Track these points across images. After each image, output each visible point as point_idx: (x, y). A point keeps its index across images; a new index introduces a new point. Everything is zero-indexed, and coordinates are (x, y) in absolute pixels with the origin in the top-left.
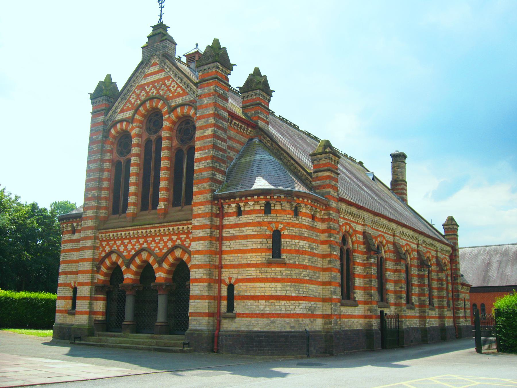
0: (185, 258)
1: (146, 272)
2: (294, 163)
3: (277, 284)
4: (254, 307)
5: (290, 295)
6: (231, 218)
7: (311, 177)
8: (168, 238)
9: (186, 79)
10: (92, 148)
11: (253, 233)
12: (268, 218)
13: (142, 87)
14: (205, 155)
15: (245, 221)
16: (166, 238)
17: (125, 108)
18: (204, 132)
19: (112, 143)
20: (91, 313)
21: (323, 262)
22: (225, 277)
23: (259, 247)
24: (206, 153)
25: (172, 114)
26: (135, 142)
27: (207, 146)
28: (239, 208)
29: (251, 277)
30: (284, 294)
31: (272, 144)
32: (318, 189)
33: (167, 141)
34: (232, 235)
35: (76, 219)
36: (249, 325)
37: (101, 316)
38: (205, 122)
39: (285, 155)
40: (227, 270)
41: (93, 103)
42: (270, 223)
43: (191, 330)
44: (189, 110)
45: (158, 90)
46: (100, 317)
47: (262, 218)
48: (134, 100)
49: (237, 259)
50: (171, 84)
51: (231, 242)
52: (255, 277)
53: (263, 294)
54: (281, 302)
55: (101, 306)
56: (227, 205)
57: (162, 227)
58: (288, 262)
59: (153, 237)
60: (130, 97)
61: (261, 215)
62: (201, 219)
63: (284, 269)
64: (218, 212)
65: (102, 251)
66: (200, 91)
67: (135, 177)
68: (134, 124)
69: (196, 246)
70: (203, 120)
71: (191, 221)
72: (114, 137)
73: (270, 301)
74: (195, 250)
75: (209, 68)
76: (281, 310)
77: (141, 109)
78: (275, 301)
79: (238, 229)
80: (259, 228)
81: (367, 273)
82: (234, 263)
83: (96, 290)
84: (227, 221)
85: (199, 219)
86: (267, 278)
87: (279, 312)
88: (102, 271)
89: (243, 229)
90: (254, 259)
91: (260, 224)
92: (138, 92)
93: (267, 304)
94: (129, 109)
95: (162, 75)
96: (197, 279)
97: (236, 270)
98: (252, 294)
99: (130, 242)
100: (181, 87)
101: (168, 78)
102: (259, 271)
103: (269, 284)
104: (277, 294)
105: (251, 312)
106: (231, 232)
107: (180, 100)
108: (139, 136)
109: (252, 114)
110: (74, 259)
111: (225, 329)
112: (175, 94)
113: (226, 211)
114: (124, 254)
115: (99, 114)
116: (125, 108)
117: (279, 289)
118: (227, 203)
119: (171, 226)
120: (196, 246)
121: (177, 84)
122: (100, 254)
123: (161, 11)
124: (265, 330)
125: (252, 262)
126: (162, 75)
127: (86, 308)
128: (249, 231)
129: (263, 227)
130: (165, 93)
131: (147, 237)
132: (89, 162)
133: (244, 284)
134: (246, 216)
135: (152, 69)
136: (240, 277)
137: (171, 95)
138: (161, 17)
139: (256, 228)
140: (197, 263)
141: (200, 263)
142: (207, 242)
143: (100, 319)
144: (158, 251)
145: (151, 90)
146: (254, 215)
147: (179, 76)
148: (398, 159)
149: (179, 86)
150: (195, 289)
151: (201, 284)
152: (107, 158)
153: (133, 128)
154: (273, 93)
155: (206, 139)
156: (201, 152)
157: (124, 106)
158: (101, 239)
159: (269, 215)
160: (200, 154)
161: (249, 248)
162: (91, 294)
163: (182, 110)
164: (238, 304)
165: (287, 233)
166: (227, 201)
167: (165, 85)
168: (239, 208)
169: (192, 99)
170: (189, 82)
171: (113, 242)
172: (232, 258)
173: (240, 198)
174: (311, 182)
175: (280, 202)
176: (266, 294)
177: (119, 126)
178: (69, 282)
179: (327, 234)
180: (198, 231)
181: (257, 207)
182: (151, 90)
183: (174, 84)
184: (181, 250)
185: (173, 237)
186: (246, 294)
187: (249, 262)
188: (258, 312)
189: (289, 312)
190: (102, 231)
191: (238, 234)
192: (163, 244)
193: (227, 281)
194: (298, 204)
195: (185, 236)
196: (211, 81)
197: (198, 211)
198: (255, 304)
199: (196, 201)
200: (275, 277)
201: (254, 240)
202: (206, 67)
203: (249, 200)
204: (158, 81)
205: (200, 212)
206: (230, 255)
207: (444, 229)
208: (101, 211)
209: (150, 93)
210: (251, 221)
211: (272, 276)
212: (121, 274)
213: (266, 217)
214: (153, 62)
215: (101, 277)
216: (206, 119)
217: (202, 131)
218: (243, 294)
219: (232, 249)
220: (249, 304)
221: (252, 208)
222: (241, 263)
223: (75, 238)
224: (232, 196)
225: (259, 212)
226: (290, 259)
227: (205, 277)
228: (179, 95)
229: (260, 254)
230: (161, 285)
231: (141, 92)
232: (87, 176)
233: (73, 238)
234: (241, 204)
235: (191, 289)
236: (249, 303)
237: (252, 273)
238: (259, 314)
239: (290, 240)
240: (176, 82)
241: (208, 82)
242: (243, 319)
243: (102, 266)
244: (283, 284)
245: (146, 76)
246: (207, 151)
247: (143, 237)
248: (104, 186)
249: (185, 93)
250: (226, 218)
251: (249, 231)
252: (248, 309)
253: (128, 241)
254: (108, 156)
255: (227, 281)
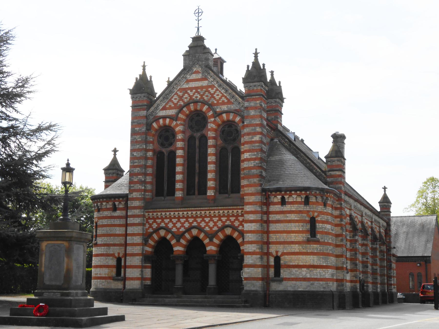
0: (235, 235)
1: (196, 245)
2: (310, 162)
3: (314, 256)
4: (298, 273)
5: (323, 264)
6: (276, 206)
7: (326, 174)
8: (217, 219)
9: (232, 91)
10: (135, 139)
11: (296, 219)
12: (307, 208)
13: (185, 91)
14: (254, 157)
15: (289, 210)
16: (215, 219)
17: (167, 106)
18: (252, 138)
19: (154, 135)
20: (142, 279)
21: (336, 240)
22: (272, 251)
23: (301, 229)
24: (254, 155)
25: (217, 118)
26: (180, 138)
27: (255, 150)
28: (283, 198)
29: (296, 251)
30: (319, 264)
31: (290, 145)
32: (332, 184)
33: (213, 140)
34: (278, 219)
35: (119, 199)
36: (294, 287)
37: (149, 282)
38: (252, 130)
39: (302, 154)
40: (274, 245)
41: (132, 98)
42: (308, 212)
43: (246, 291)
44: (235, 117)
45: (202, 96)
46: (148, 282)
47: (302, 207)
48: (177, 100)
49: (283, 237)
50: (215, 92)
51: (277, 224)
52: (298, 251)
53: (305, 264)
54: (317, 269)
55: (149, 273)
56: (273, 197)
57: (212, 210)
58: (321, 241)
59: (203, 218)
60: (172, 98)
61: (302, 206)
62: (252, 206)
63: (318, 246)
64: (265, 201)
65: (149, 228)
66: (246, 104)
67: (181, 167)
68: (179, 122)
69: (247, 227)
70: (251, 128)
71: (242, 207)
72: (156, 130)
73: (310, 269)
74: (247, 230)
75: (255, 86)
76: (317, 276)
77: (185, 109)
78: (313, 269)
79: (283, 215)
80: (301, 215)
81: (353, 247)
82: (280, 240)
83: (145, 260)
84: (273, 208)
85: (250, 206)
86: (307, 252)
87: (316, 277)
88: (150, 244)
89: (288, 215)
90: (297, 238)
91: (301, 212)
92: (181, 94)
93: (308, 271)
94: (171, 108)
95: (205, 83)
96: (250, 252)
97: (282, 245)
98: (296, 264)
99: (179, 221)
100: (226, 97)
101: (212, 87)
102: (301, 247)
103: (309, 256)
104: (314, 264)
105: (296, 277)
106: (276, 217)
107: (225, 108)
108: (183, 132)
109: (272, 118)
110: (117, 233)
111: (274, 289)
112: (220, 102)
113: (272, 201)
114: (173, 230)
115: (140, 109)
116: (167, 106)
117: (316, 260)
118: (273, 195)
119: (221, 210)
120: (247, 227)
121: (221, 93)
122: (147, 229)
123: (198, 24)
124: (307, 290)
125: (295, 240)
126: (205, 83)
127: (138, 275)
128: (293, 217)
129: (304, 215)
130: (209, 100)
131: (197, 217)
132: (132, 151)
133: (289, 256)
134: (289, 206)
135: (194, 76)
136: (285, 251)
137: (216, 102)
138: (198, 29)
139: (298, 215)
140: (250, 240)
141: (253, 240)
142: (259, 224)
143: (149, 284)
144: (209, 229)
145: (194, 94)
146: (297, 205)
147: (224, 87)
148: (339, 139)
149: (223, 96)
150: (248, 260)
151: (254, 256)
152: (150, 148)
153: (177, 125)
154: (285, 100)
155: (254, 143)
156: (250, 153)
157: (167, 104)
158: (147, 217)
159: (308, 206)
160: (249, 155)
161: (293, 229)
162: (142, 263)
163: (228, 117)
164: (285, 271)
165: (320, 219)
166: (273, 193)
167: (209, 92)
168: (283, 198)
169: (237, 108)
170: (234, 93)
171: (160, 220)
172: (278, 237)
173: (286, 192)
174: (324, 178)
175: (315, 196)
176: (307, 264)
177: (161, 121)
178: (112, 253)
179: (339, 219)
180: (250, 215)
181: (299, 199)
182: (194, 94)
183: (218, 93)
184: (231, 229)
185: (222, 218)
186: (291, 264)
187: (293, 240)
188: (301, 277)
189: (322, 277)
190: (149, 210)
191: (283, 219)
192: (213, 224)
193: (274, 254)
194: (327, 197)
195: (234, 218)
196: (257, 97)
197: (249, 200)
198: (299, 271)
199: (247, 192)
200: (313, 251)
201: (297, 224)
202: (251, 84)
203: (293, 194)
204: (202, 88)
205: (251, 201)
206: (277, 235)
207: (380, 206)
208: (147, 194)
209: (193, 97)
210: (294, 209)
211: (311, 251)
212: (171, 247)
213: (305, 207)
214: (195, 70)
215: (149, 249)
216: (253, 128)
217: (251, 136)
218: (289, 264)
219: (278, 230)
220: (294, 271)
221: (295, 200)
222: (286, 240)
223: (117, 215)
224: (279, 190)
225: (300, 203)
226: (322, 239)
227: (258, 251)
228: (223, 103)
229: (302, 235)
230: (213, 256)
231: (184, 95)
232: (131, 162)
233: (114, 215)
234: (286, 197)
235: (245, 260)
236: (294, 270)
237: (296, 248)
238: (302, 278)
239: (322, 225)
240: (220, 92)
241: (254, 97)
242: (289, 282)
243: (150, 240)
244: (318, 256)
245: (188, 81)
246: (255, 153)
247: (192, 217)
248: (148, 172)
249: (229, 102)
250: (272, 206)
251: (293, 217)
252: (293, 275)
253: (177, 220)
254: (151, 147)
255: (274, 254)
